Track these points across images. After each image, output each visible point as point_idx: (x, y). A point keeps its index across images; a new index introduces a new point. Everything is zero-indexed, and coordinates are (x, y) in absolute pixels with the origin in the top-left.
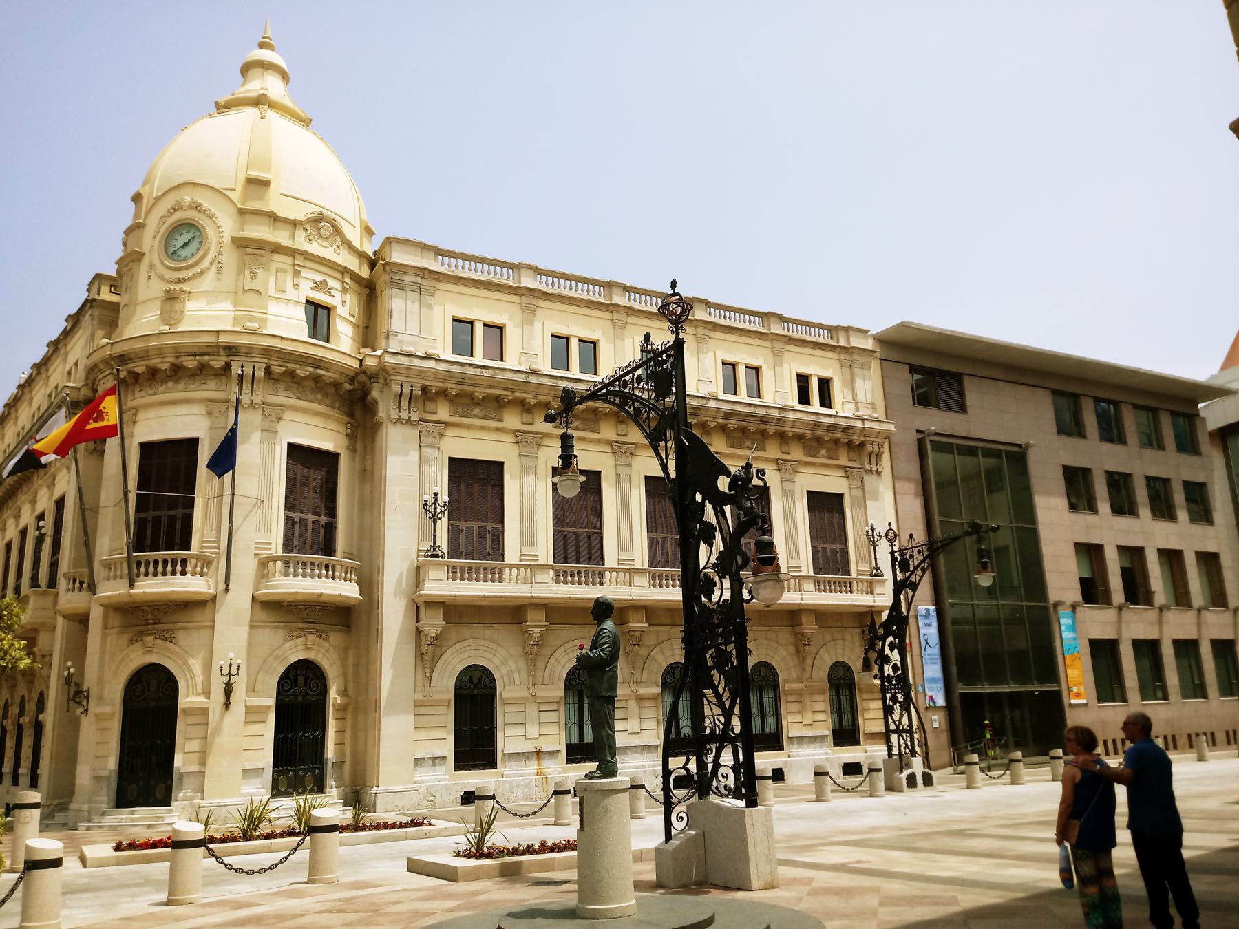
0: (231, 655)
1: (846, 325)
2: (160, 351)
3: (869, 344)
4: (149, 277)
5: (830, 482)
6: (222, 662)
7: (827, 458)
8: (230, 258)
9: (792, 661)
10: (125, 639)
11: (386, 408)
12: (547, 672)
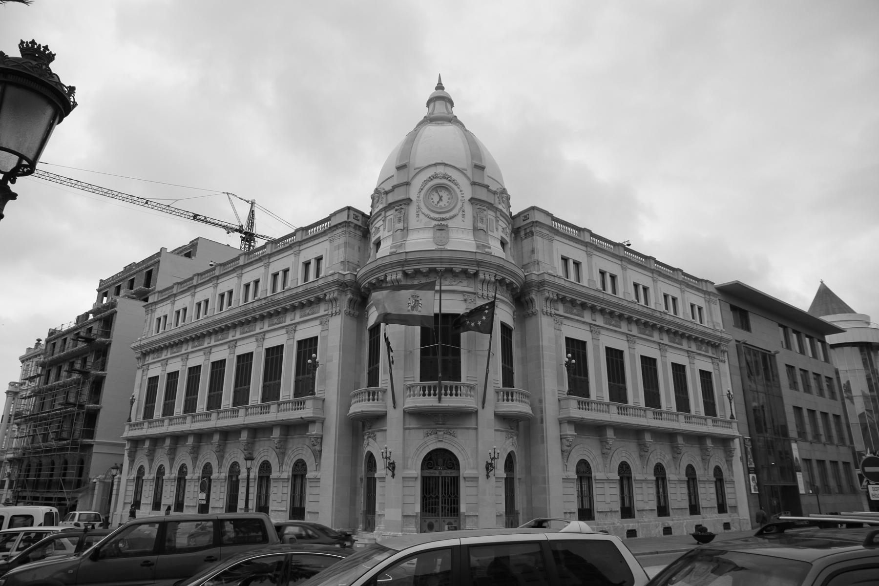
0: (495, 447)
1: (706, 279)
2: (441, 260)
3: (711, 289)
4: (418, 216)
5: (708, 367)
6: (490, 451)
7: (705, 352)
8: (469, 209)
9: (701, 464)
10: (421, 433)
11: (539, 303)
12: (612, 465)
